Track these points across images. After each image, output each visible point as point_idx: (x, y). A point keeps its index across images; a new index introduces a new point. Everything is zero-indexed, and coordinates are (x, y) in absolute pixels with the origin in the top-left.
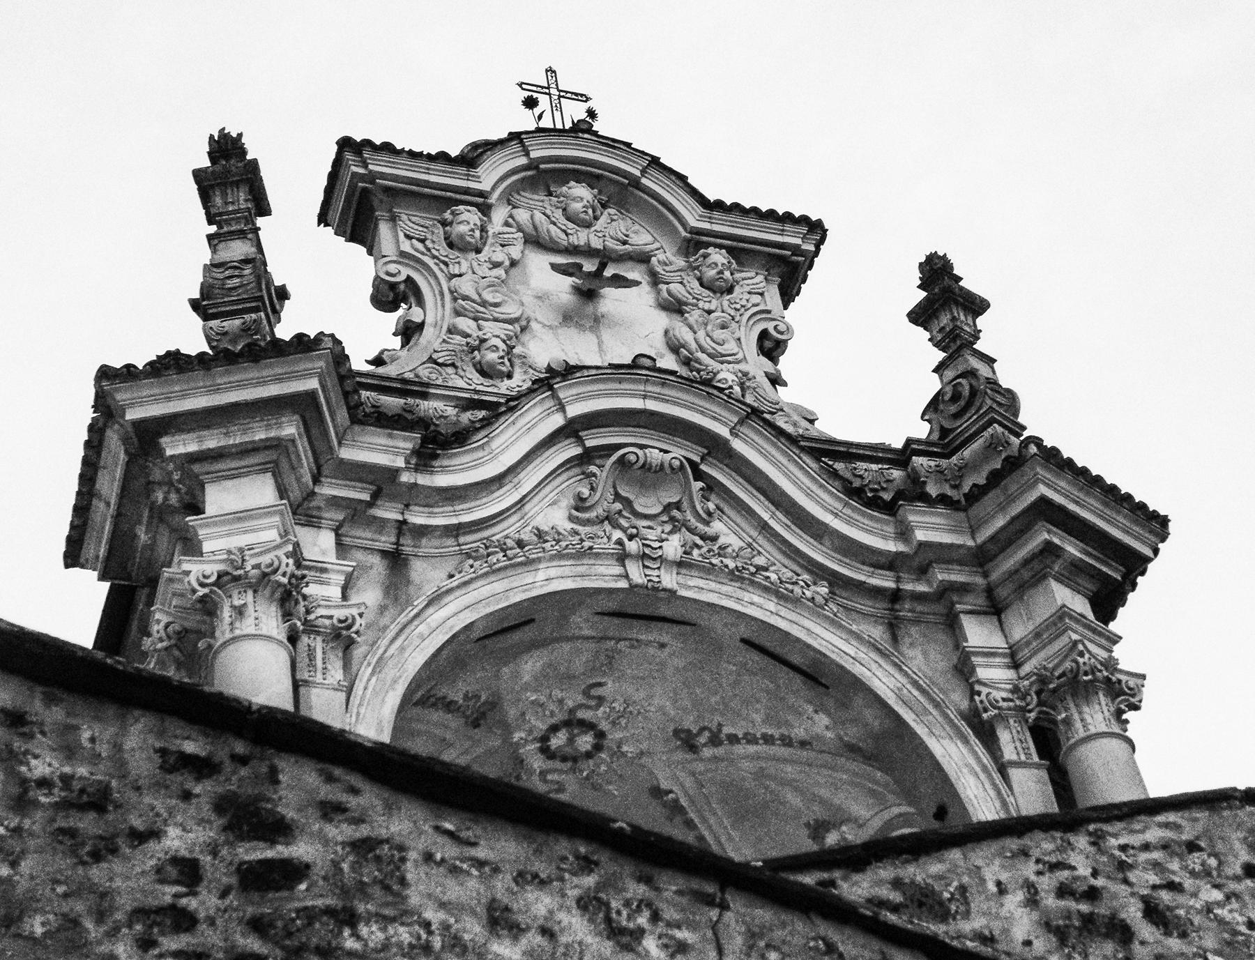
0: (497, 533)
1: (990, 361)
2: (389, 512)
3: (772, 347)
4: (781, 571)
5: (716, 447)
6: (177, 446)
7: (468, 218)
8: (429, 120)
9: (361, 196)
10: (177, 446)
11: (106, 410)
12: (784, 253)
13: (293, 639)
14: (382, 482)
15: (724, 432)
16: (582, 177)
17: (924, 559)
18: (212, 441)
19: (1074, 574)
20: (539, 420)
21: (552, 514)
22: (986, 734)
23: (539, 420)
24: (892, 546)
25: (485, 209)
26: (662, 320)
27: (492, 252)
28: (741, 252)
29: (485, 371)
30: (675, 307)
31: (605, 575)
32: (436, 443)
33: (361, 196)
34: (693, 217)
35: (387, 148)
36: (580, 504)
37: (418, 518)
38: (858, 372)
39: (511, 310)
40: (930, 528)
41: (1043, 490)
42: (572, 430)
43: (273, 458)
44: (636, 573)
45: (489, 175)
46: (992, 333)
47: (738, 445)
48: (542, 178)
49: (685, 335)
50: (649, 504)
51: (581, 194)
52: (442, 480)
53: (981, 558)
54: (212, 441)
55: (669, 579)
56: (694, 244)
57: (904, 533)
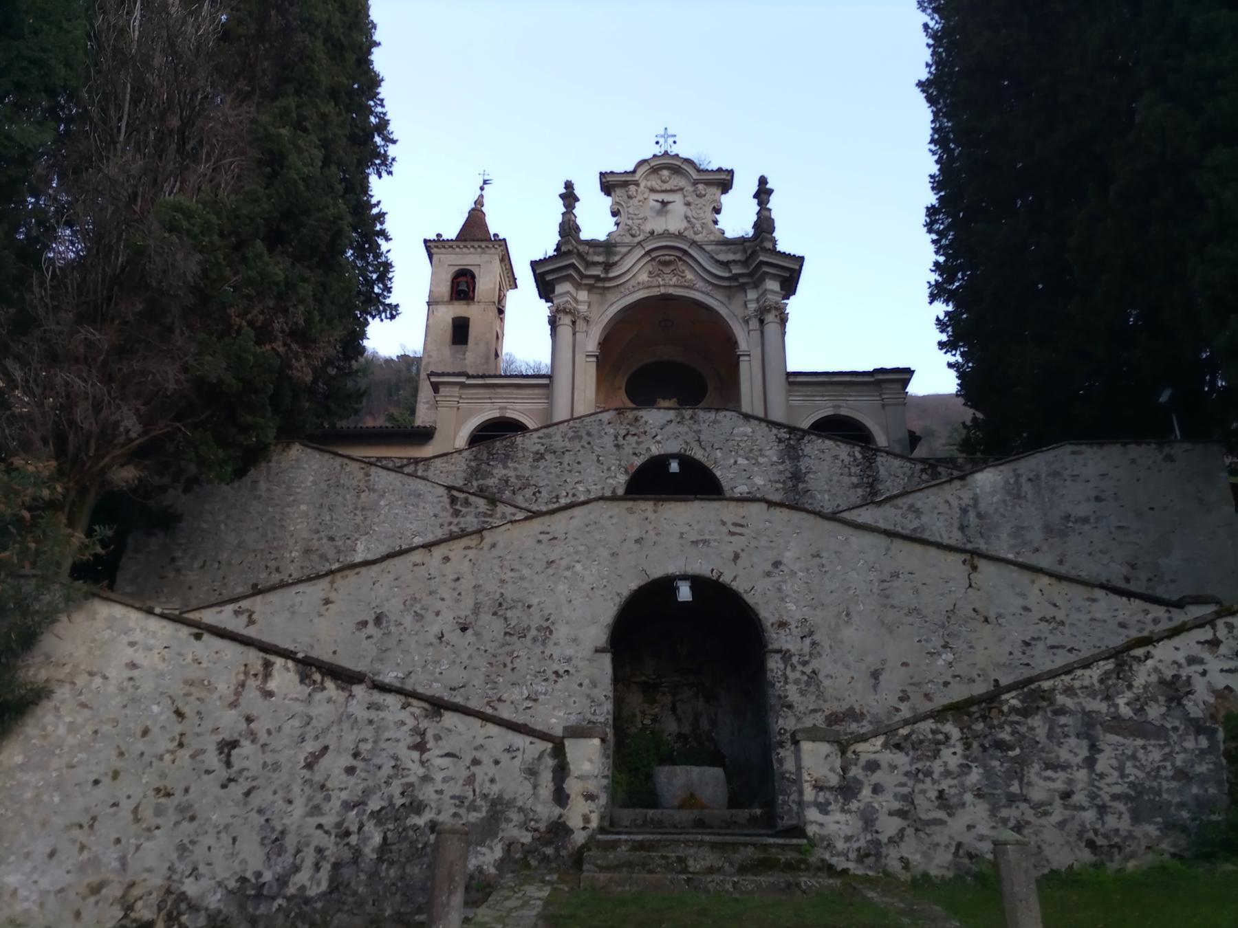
0: (627, 286)
1: (770, 210)
2: (600, 285)
3: (717, 211)
4: (700, 284)
5: (685, 252)
6: (549, 278)
7: (632, 188)
8: (623, 163)
9: (609, 183)
10: (549, 278)
11: (534, 270)
12: (724, 180)
13: (574, 323)
14: (597, 278)
15: (686, 247)
16: (668, 166)
17: (735, 277)
18: (555, 276)
19: (774, 277)
20: (639, 253)
21: (644, 277)
22: (747, 322)
23: (639, 253)
24: (727, 275)
25: (637, 184)
26: (685, 209)
27: (640, 197)
28: (709, 183)
29: (633, 236)
30: (688, 204)
31: (655, 292)
32: (608, 266)
33: (609, 183)
34: (694, 175)
35: (612, 173)
36: (650, 273)
37: (607, 285)
38: (736, 217)
39: (641, 216)
40: (736, 270)
41: (761, 258)
42: (648, 253)
43: (568, 278)
44: (663, 290)
45: (637, 176)
46: (774, 203)
47: (691, 251)
48: (655, 170)
49: (689, 214)
50: (667, 270)
51: (665, 173)
52: (611, 275)
53: (751, 275)
54: (555, 276)
55: (671, 291)
56: (695, 183)
57: (730, 271)
